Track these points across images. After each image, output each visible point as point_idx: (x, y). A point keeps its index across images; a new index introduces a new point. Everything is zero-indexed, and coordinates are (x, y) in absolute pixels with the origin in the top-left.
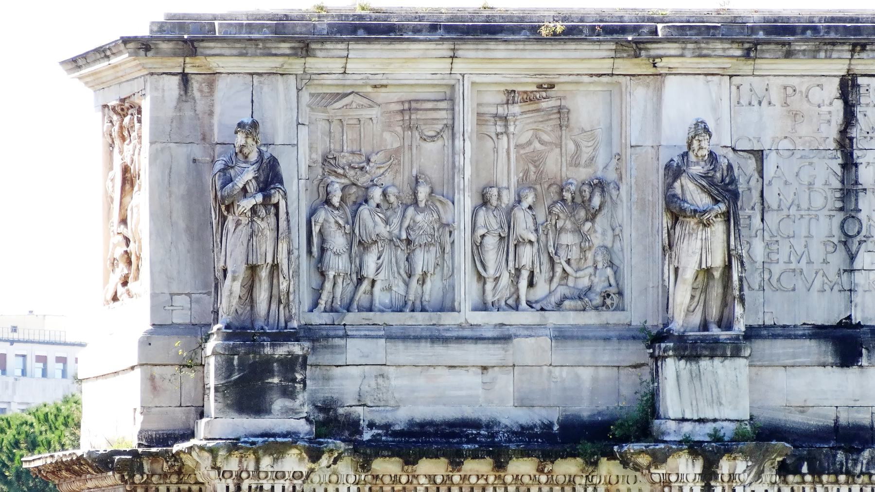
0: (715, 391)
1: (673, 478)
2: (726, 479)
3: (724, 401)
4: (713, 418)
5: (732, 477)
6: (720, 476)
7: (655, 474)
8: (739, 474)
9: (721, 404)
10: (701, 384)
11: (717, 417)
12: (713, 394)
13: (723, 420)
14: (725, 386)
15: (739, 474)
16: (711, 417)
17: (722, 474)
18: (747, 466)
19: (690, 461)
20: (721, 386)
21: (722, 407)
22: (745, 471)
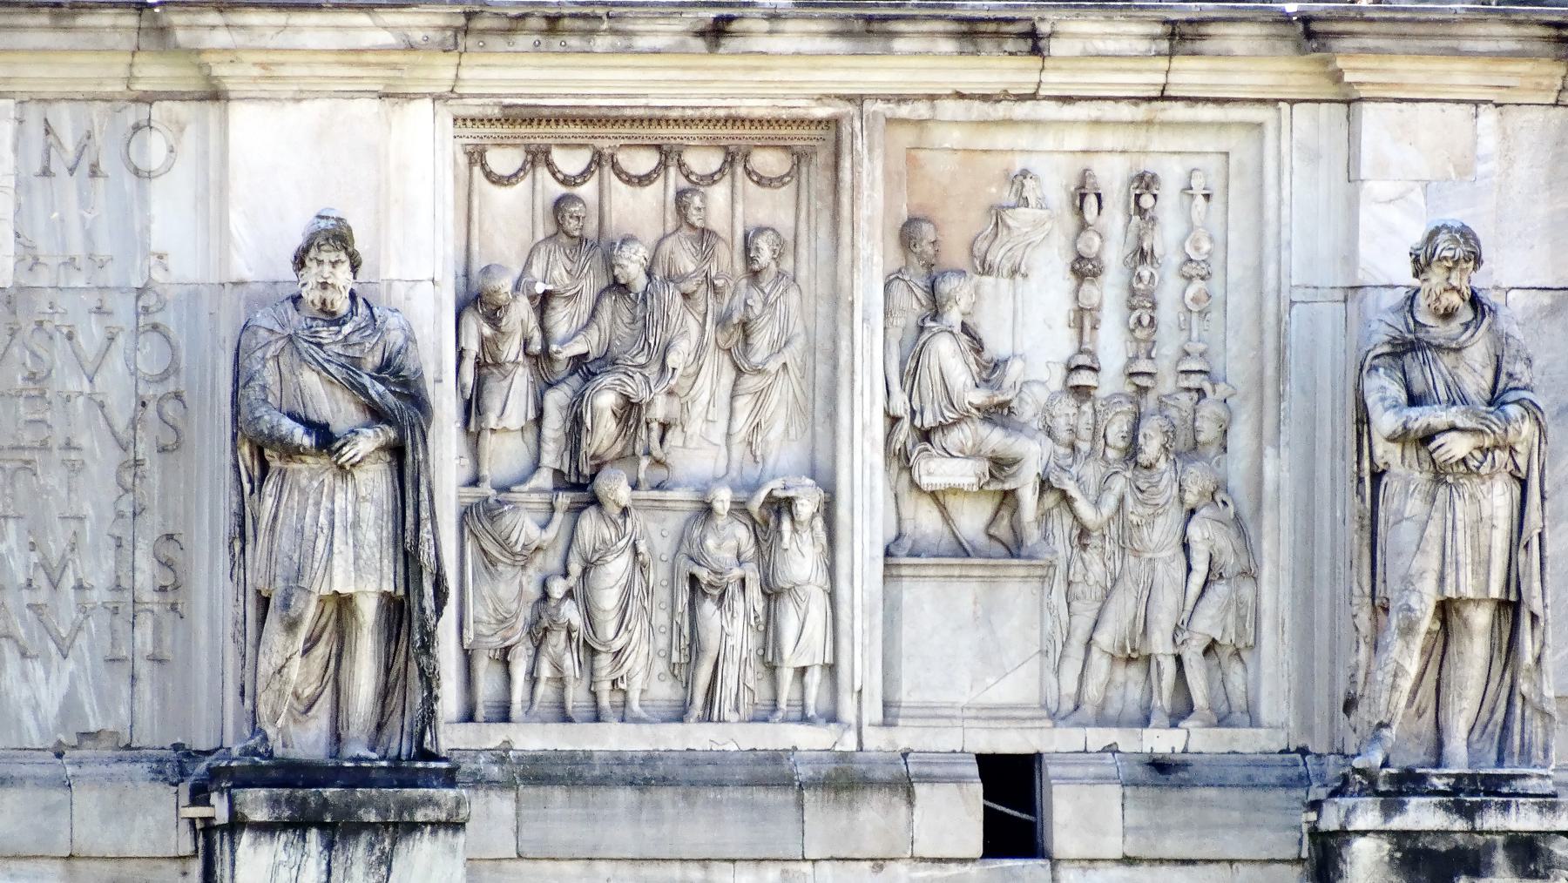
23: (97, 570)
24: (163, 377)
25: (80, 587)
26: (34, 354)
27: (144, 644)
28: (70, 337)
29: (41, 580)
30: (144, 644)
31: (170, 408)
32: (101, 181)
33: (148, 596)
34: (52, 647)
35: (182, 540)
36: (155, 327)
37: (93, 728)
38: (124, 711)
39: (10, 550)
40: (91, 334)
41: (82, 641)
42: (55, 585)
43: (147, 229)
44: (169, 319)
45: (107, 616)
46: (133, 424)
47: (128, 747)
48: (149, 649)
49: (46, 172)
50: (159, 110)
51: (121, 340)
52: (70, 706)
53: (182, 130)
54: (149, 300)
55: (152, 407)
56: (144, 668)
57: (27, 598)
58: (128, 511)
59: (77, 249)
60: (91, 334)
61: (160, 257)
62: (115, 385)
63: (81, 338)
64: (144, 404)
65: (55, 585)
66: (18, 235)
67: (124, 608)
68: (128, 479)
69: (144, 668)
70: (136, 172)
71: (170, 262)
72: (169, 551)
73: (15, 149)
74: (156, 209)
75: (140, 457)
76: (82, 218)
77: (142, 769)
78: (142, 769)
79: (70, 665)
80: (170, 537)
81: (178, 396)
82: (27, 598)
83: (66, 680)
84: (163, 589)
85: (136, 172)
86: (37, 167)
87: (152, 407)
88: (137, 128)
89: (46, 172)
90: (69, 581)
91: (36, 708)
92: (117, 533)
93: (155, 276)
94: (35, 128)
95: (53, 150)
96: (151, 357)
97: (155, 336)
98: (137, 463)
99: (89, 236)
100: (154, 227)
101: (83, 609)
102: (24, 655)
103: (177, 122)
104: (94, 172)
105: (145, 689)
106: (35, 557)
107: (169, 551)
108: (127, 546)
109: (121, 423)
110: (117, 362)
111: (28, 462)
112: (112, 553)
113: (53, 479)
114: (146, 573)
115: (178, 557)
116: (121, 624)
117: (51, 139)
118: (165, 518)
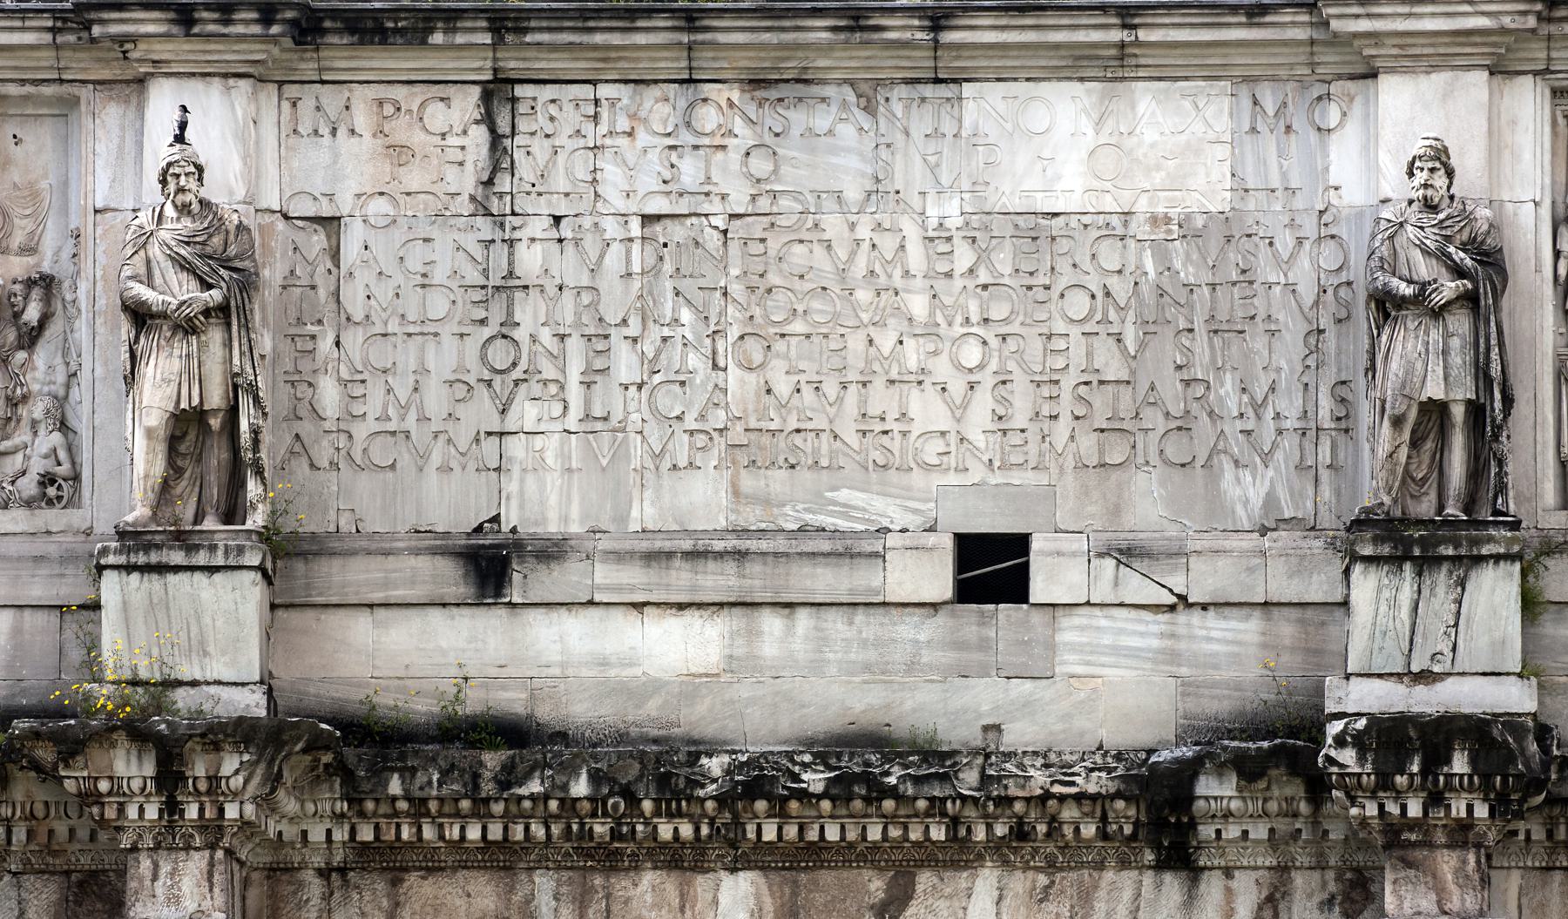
0: (194, 630)
1: (104, 786)
2: (203, 786)
3: (211, 649)
4: (190, 679)
5: (214, 779)
6: (190, 781)
7: (69, 777)
8: (228, 778)
9: (206, 654)
10: (169, 617)
11: (198, 676)
12: (192, 635)
13: (208, 683)
14: (214, 620)
15: (228, 778)
16: (187, 677)
17: (195, 778)
18: (242, 763)
19: (134, 753)
20: (207, 620)
21: (207, 660)
22: (237, 772)
23: (1290, 406)
24: (1340, 268)
25: (1277, 416)
26: (1244, 257)
27: (1324, 458)
28: (1271, 244)
29: (1251, 413)
30: (1324, 458)
31: (1343, 292)
32: (1293, 136)
33: (1327, 424)
34: (1258, 460)
35: (1352, 385)
36: (1333, 237)
37: (1287, 516)
38: (1309, 504)
39: (1227, 393)
40: (1285, 242)
41: (1279, 456)
42: (1259, 417)
43: (1327, 169)
44: (1342, 230)
45: (1296, 438)
46: (1317, 303)
47: (1313, 529)
48: (1328, 461)
49: (1253, 130)
50: (1335, 88)
51: (1307, 245)
52: (1270, 501)
53: (1352, 100)
54: (1326, 218)
55: (1330, 291)
56: (1325, 475)
57: (1239, 425)
58: (1313, 365)
59: (1275, 183)
60: (1285, 242)
61: (1336, 189)
62: (1304, 275)
63: (1278, 244)
64: (1325, 291)
65: (1259, 417)
66: (1233, 175)
67: (1308, 431)
68: (1312, 341)
69: (1325, 475)
70: (1319, 129)
71: (1342, 192)
72: (1342, 391)
73: (1231, 115)
74: (1333, 156)
75: (1321, 327)
76: (1280, 163)
77: (1319, 543)
78: (1319, 543)
79: (1270, 473)
80: (1344, 383)
81: (1349, 284)
82: (1239, 425)
83: (1267, 483)
84: (1339, 419)
85: (1319, 129)
86: (1247, 127)
87: (1330, 291)
88: (1320, 98)
89: (1253, 130)
90: (1270, 414)
91: (1246, 502)
92: (1305, 379)
93: (1332, 202)
94: (1246, 103)
95: (1259, 117)
96: (1329, 257)
97: (1332, 243)
98: (1321, 332)
99: (1284, 176)
100: (1332, 168)
101: (1280, 432)
102: (1236, 462)
103: (1349, 95)
104: (1288, 128)
105: (1326, 492)
106: (1245, 398)
107: (1342, 391)
108: (1312, 388)
109: (1308, 300)
110: (1304, 262)
111: (1241, 332)
112: (1300, 394)
113: (1259, 343)
114: (1326, 405)
115: (1350, 397)
116: (1309, 446)
117: (1258, 107)
118: (1339, 370)
